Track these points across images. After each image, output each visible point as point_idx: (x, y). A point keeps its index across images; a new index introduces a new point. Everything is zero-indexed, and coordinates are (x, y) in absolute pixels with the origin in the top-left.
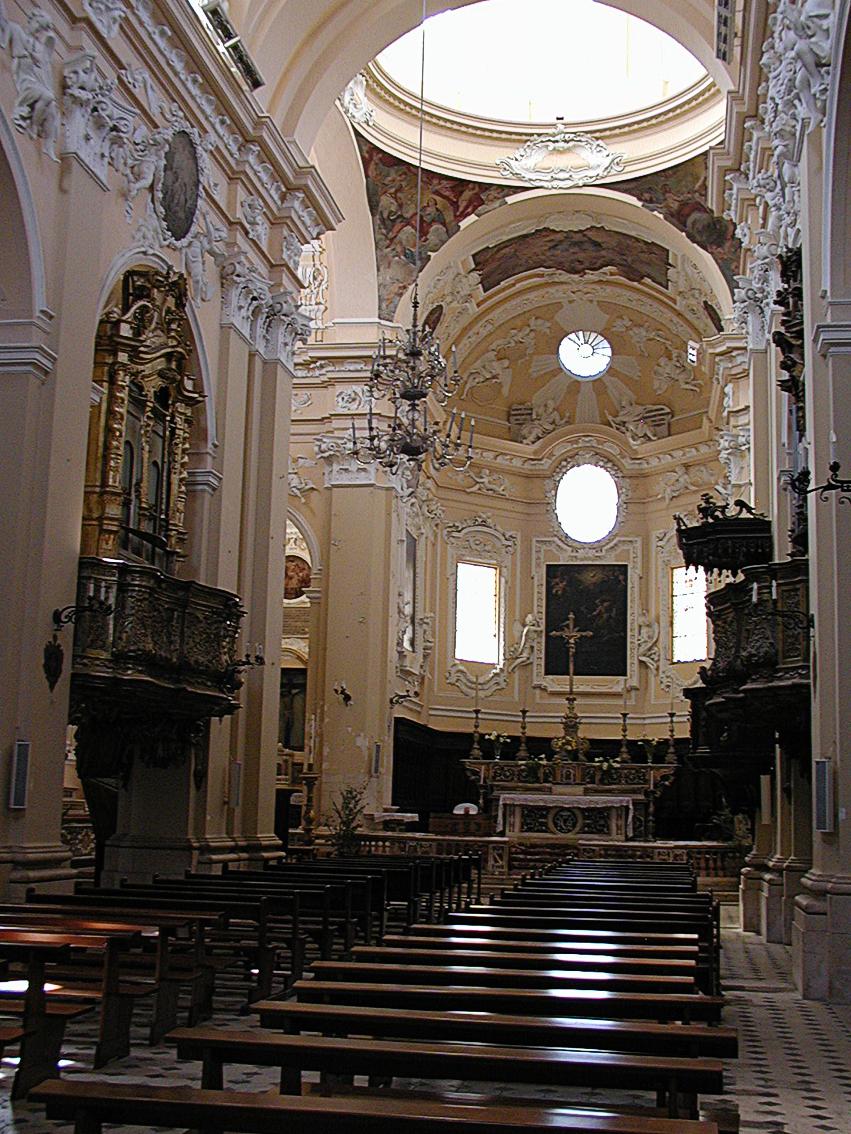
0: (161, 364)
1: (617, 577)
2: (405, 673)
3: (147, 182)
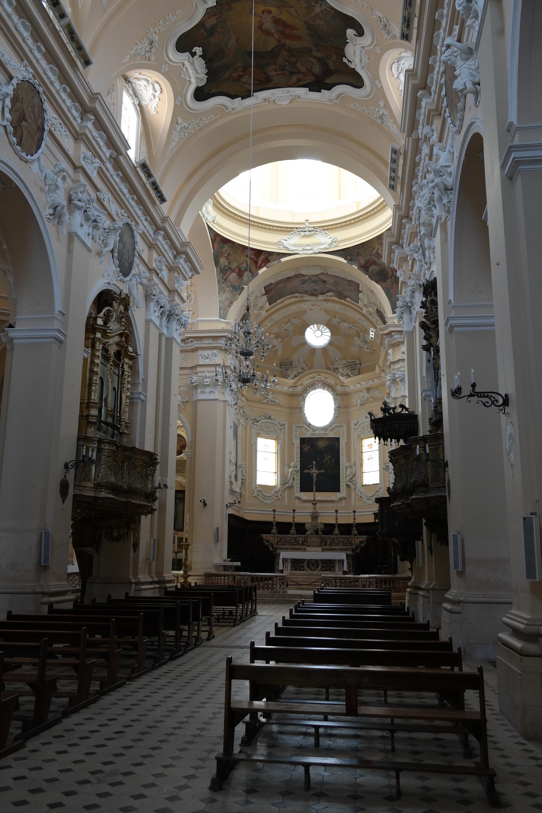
0: (117, 339)
2: (233, 492)
3: (110, 248)
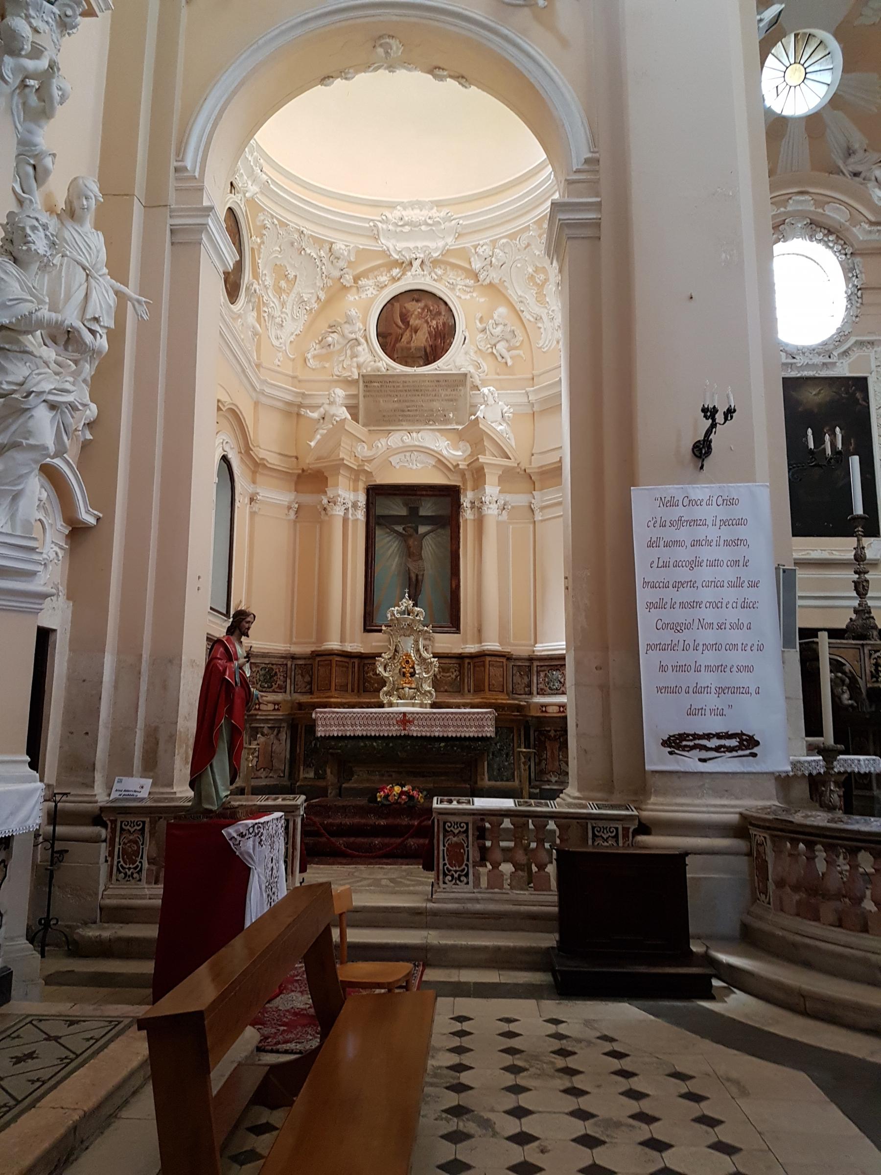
1: (854, 394)
